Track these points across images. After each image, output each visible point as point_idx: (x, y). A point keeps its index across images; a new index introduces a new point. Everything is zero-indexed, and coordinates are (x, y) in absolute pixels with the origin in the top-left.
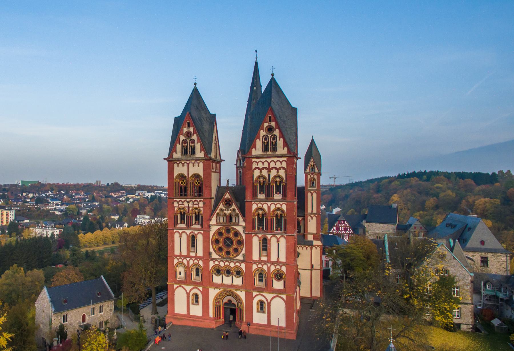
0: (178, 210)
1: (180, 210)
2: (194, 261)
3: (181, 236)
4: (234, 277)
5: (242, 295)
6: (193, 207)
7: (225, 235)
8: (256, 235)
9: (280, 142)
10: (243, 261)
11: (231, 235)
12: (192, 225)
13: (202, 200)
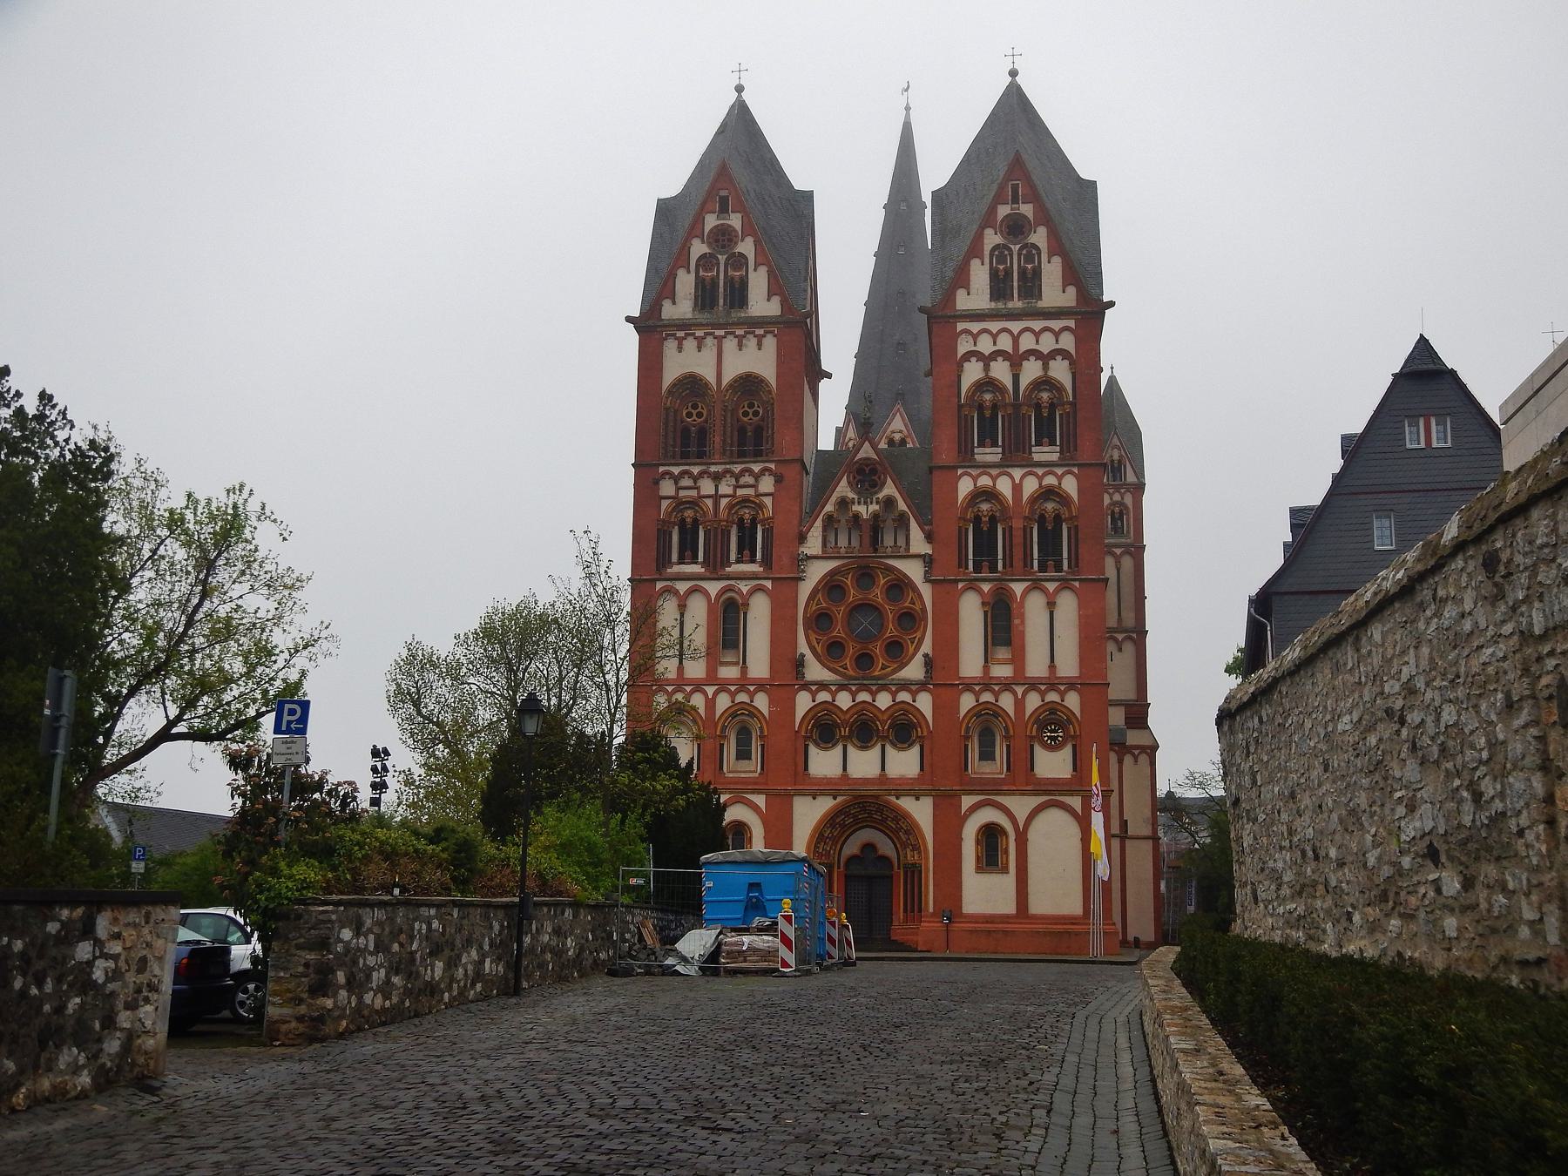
1: (682, 511)
2: (733, 695)
4: (889, 748)
5: (921, 812)
6: (733, 496)
7: (853, 595)
8: (972, 585)
9: (1052, 272)
10: (922, 686)
11: (877, 594)
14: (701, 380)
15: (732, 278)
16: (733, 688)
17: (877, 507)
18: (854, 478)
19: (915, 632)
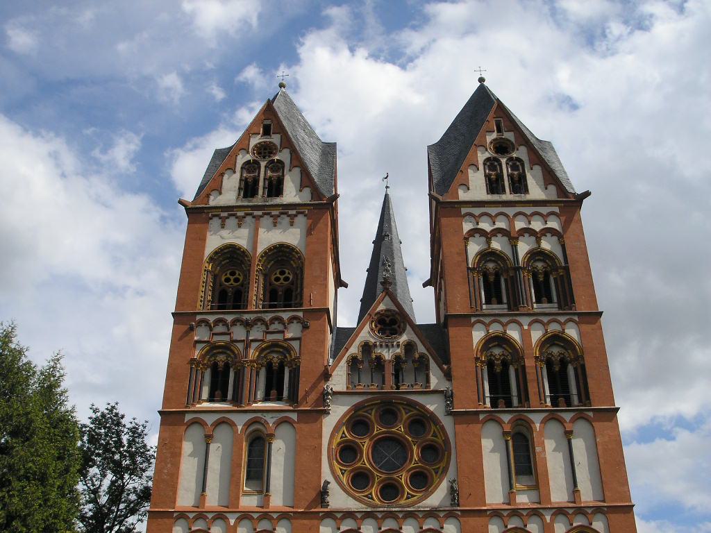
0: (207, 353)
1: (215, 355)
7: (378, 430)
8: (492, 418)
10: (450, 514)
12: (256, 402)
14: (239, 249)
15: (270, 177)
17: (398, 351)
18: (376, 326)
19: (441, 461)
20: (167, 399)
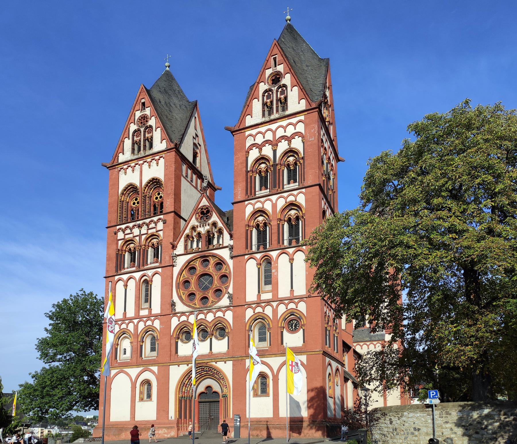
2: (145, 322)
3: (127, 286)
13: (162, 217)
16: (145, 319)
20: (107, 271)
